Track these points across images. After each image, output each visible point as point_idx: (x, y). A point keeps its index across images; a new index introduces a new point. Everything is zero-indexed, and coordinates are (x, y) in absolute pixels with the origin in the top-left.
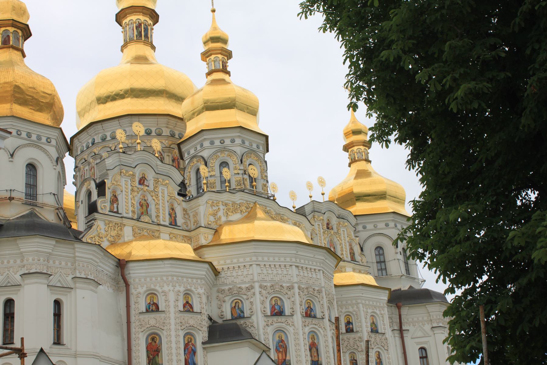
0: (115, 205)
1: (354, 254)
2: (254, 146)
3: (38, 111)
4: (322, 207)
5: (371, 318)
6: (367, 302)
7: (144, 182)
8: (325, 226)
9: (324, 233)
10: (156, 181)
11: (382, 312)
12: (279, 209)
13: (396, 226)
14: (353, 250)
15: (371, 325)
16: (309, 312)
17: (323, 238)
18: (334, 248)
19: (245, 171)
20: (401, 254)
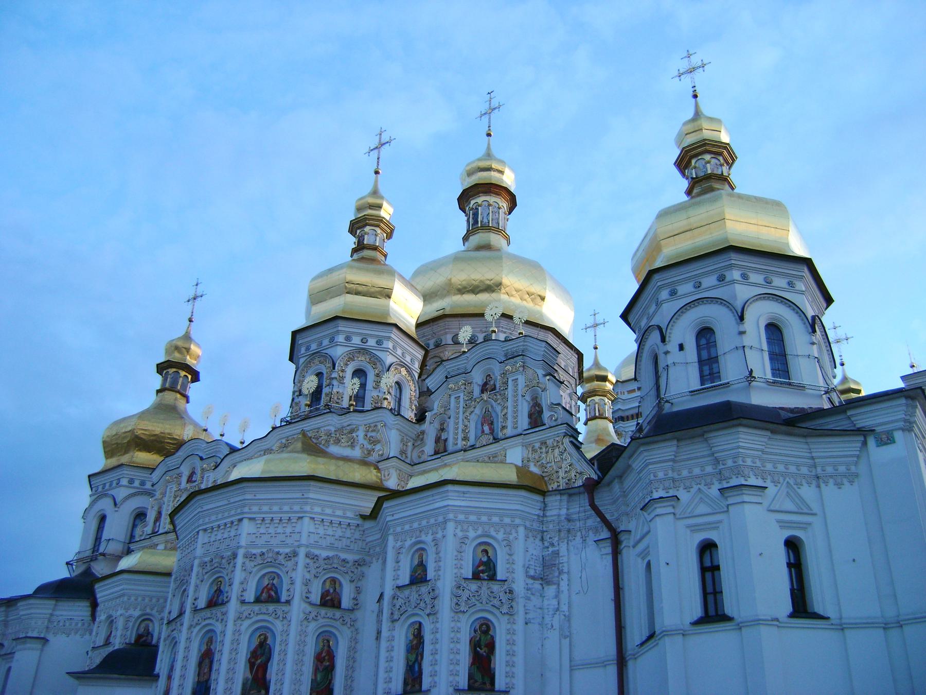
0: (158, 524)
1: (541, 412)
2: (326, 342)
3: (124, 454)
4: (465, 361)
5: (417, 556)
6: (407, 527)
7: (192, 476)
8: (477, 391)
9: (467, 407)
10: (203, 470)
11: (439, 535)
12: (340, 420)
13: (673, 293)
14: (539, 405)
15: (413, 571)
16: (215, 598)
17: (461, 416)
18: (492, 423)
19: (300, 391)
20: (681, 347)
